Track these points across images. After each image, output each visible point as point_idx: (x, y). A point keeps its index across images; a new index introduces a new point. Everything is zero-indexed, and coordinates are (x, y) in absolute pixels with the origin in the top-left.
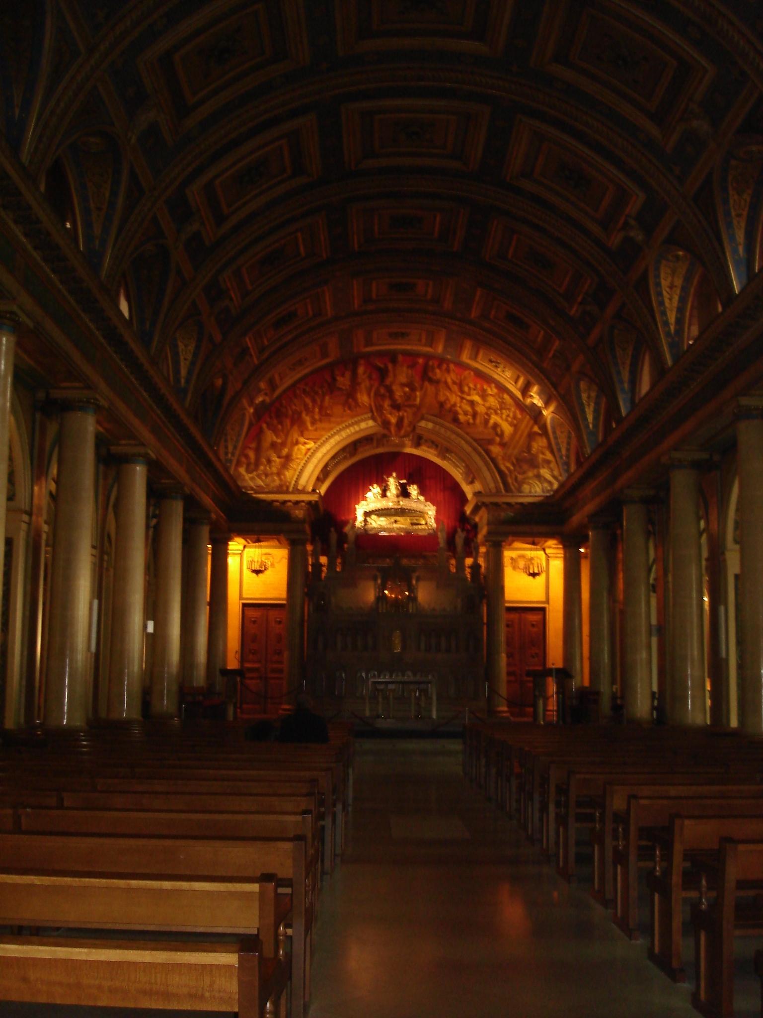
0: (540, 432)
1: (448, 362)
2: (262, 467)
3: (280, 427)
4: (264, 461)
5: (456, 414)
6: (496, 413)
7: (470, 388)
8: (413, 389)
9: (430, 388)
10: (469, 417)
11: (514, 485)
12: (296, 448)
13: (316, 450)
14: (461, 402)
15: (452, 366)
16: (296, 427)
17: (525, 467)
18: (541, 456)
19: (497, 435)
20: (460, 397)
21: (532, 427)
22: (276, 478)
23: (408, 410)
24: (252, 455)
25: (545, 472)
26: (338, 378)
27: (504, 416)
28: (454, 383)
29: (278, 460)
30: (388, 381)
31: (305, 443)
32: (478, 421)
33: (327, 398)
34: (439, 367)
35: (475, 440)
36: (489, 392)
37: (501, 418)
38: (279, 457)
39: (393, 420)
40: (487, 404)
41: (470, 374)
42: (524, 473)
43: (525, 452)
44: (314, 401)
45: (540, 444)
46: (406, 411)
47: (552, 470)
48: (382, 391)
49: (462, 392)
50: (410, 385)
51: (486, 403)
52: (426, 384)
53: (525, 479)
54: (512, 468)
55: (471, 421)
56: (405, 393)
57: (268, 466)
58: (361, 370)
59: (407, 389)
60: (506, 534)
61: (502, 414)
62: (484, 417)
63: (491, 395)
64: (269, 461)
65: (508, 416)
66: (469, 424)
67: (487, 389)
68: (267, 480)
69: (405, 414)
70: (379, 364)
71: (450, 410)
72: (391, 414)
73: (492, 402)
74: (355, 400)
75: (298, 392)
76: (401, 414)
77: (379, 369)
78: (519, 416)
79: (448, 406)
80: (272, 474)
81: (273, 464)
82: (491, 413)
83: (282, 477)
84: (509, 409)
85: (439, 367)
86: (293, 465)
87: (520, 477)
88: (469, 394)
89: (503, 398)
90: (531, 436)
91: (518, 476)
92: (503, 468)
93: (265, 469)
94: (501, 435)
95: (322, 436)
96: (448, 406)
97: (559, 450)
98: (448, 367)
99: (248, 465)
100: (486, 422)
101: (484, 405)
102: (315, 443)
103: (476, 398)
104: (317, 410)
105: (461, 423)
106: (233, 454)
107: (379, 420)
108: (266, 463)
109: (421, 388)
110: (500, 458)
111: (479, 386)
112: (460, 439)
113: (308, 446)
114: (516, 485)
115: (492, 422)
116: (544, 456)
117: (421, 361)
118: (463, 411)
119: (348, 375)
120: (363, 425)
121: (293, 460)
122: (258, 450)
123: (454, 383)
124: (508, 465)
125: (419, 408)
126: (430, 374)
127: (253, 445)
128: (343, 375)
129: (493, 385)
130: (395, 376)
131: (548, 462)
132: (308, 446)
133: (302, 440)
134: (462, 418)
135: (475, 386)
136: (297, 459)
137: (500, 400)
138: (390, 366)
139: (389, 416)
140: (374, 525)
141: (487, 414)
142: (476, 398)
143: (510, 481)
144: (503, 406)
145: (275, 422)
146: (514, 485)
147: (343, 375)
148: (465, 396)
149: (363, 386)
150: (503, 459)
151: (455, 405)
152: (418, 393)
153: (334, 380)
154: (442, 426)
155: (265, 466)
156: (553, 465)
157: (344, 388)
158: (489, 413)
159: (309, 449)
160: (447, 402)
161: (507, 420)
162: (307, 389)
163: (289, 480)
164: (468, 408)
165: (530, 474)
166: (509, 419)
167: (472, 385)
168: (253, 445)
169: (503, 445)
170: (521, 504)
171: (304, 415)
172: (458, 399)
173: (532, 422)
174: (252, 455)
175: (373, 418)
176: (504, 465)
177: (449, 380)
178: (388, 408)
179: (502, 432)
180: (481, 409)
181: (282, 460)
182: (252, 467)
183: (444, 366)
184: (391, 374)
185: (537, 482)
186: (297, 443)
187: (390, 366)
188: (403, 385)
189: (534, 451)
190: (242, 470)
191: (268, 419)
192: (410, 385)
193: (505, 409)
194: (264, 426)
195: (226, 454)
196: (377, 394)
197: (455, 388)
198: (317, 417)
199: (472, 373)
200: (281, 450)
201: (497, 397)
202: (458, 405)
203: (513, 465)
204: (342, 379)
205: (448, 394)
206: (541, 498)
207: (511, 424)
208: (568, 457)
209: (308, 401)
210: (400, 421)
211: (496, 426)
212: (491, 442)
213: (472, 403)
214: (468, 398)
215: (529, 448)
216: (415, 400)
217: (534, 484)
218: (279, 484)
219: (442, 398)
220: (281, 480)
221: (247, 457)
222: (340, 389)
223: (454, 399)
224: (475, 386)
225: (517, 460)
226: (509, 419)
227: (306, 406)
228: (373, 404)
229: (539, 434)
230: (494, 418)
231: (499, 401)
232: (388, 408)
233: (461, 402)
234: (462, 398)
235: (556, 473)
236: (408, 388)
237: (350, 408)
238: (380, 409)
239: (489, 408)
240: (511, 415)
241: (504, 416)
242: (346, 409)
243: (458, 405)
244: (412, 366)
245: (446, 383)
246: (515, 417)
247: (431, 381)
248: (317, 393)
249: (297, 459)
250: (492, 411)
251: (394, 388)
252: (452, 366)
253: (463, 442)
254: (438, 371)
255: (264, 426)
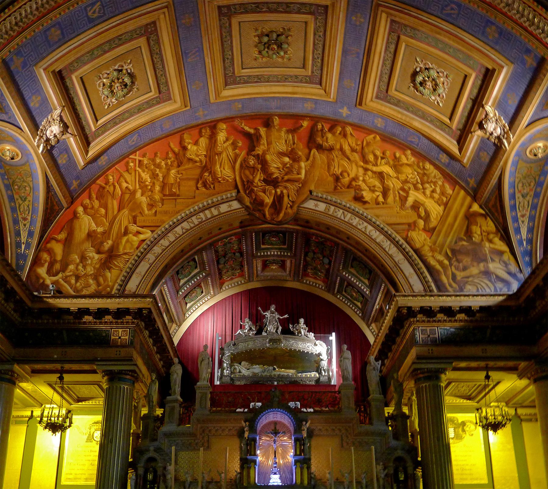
0: (482, 211)
1: (344, 124)
2: (72, 267)
3: (103, 211)
4: (76, 257)
5: (359, 188)
6: (416, 189)
7: (376, 157)
8: (296, 159)
9: (319, 157)
10: (377, 193)
11: (451, 285)
12: (125, 239)
13: (155, 242)
14: (365, 174)
15: (349, 129)
16: (126, 212)
17: (466, 260)
18: (487, 244)
19: (420, 217)
20: (362, 167)
21: (470, 207)
22: (91, 281)
23: (288, 185)
24: (58, 249)
25: (496, 267)
26: (189, 147)
27: (428, 192)
28: (353, 150)
29: (97, 256)
30: (259, 150)
31: (138, 233)
32: (390, 199)
33: (173, 172)
34: (331, 130)
35: (389, 225)
36: (404, 160)
37: (424, 193)
38: (99, 252)
39: (268, 200)
40: (403, 177)
41: (374, 138)
42: (465, 269)
43: (461, 239)
44: (154, 176)
45: (484, 228)
46: (286, 188)
47: (506, 264)
48: (252, 162)
49: (366, 161)
50: (292, 155)
51: (400, 175)
52: (314, 151)
53: (468, 277)
54: (446, 262)
55: (381, 199)
56: (284, 164)
57: (81, 264)
58: (221, 136)
59: (287, 159)
60: (449, 359)
61: (424, 189)
62: (399, 193)
63: (407, 164)
64: (83, 258)
65: (433, 191)
66: (378, 203)
67: (400, 157)
68: (78, 284)
69: (285, 191)
70: (247, 128)
71: (349, 186)
72: (264, 192)
73: (409, 173)
74: (213, 173)
75: (132, 164)
76: (279, 191)
77: (248, 135)
78: (449, 191)
79: (346, 180)
80: (86, 275)
81: (89, 262)
82: (410, 188)
83: (101, 280)
84: (435, 183)
85: (331, 130)
86: (119, 263)
87: (460, 275)
88: (376, 165)
89: (424, 168)
90: (470, 217)
91: (458, 273)
92: (433, 262)
93: (77, 269)
94: (427, 218)
95: (163, 222)
96: (346, 180)
97: (518, 231)
98: (343, 128)
99: (51, 264)
100: (403, 200)
101: (398, 178)
102: (152, 231)
103: (386, 169)
104: (157, 188)
105: (365, 203)
106: (28, 246)
107: (247, 201)
108: (78, 261)
109: (308, 159)
110: (427, 248)
111: (388, 153)
112: (365, 224)
113: (142, 237)
114: (454, 285)
115: (410, 201)
116: (492, 246)
117: (305, 124)
118: (368, 187)
119: (203, 142)
120: (224, 208)
121: (119, 256)
122: (68, 243)
123: (353, 150)
124: (441, 258)
125: (304, 183)
126: (319, 140)
127: (62, 236)
128: (196, 143)
129: (409, 152)
130: (269, 143)
131: (501, 253)
132: (142, 237)
133: (134, 228)
134: (367, 195)
135: (384, 153)
136: (126, 254)
137: (421, 172)
138: (263, 131)
139: (262, 194)
140: (245, 372)
141: (403, 189)
142: (386, 169)
143: (444, 279)
144: (424, 178)
145: (96, 204)
146: (451, 285)
147: (196, 143)
148: (370, 167)
149: (224, 155)
150: (432, 250)
151: (355, 179)
152: (303, 164)
153: (185, 148)
154: (336, 205)
155: (78, 265)
156: (507, 256)
157: (197, 159)
158: (406, 187)
159: (143, 241)
160: (345, 174)
161: (432, 197)
162: (146, 161)
163: (110, 284)
164: (377, 183)
165: (474, 270)
166: (436, 196)
167: (378, 153)
168: (62, 236)
169: (430, 231)
170: (467, 310)
171: (138, 194)
172: (361, 171)
173: (469, 199)
174: (58, 249)
175: (239, 199)
176: (433, 256)
177: (346, 148)
178: (259, 184)
179: (427, 213)
180: (394, 184)
181: (103, 256)
182: (57, 266)
183: (339, 129)
184: (264, 141)
185: (488, 282)
186: (126, 233)
187: (263, 131)
188: (282, 154)
189: (476, 238)
190: (42, 271)
191: (87, 201)
192: (292, 155)
193: (428, 183)
194: (80, 209)
195: (18, 245)
196: (244, 166)
197: (356, 157)
198: (157, 197)
199: (378, 138)
200: (102, 243)
201: (416, 167)
202: (361, 178)
203: (449, 259)
204: (195, 148)
205: (345, 164)
206: (501, 298)
207: (439, 202)
208: (530, 241)
209: (146, 176)
210: (279, 199)
211: (416, 207)
212: (412, 226)
213: (381, 176)
214: (375, 169)
215: (468, 233)
216: (299, 174)
217: (482, 283)
218: (95, 290)
219: (338, 171)
220: (99, 284)
221: (50, 252)
222: (190, 160)
223: (354, 171)
224: (384, 153)
225: (453, 251)
226: (436, 196)
227: (141, 182)
228: (238, 179)
229: (482, 215)
230: (413, 196)
231: (418, 173)
232: (259, 184)
233: (365, 174)
234: (366, 170)
235: (513, 268)
236: (289, 157)
237: (205, 185)
238: (248, 186)
239: (406, 182)
240: (438, 190)
241: (428, 192)
242: (199, 185)
243: (361, 178)
244: (293, 131)
245: (341, 149)
246: (443, 193)
247: (320, 148)
248: (159, 166)
249: (126, 254)
250: (412, 186)
251: (268, 157)
252: (349, 129)
253: (370, 228)
254: (329, 135)
255: (80, 209)
